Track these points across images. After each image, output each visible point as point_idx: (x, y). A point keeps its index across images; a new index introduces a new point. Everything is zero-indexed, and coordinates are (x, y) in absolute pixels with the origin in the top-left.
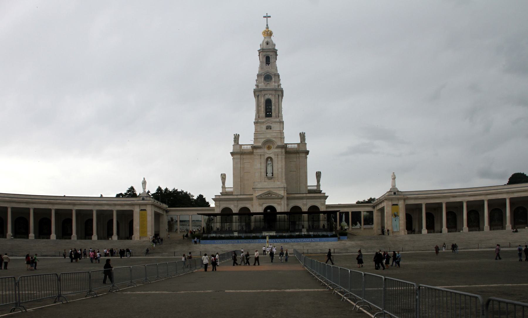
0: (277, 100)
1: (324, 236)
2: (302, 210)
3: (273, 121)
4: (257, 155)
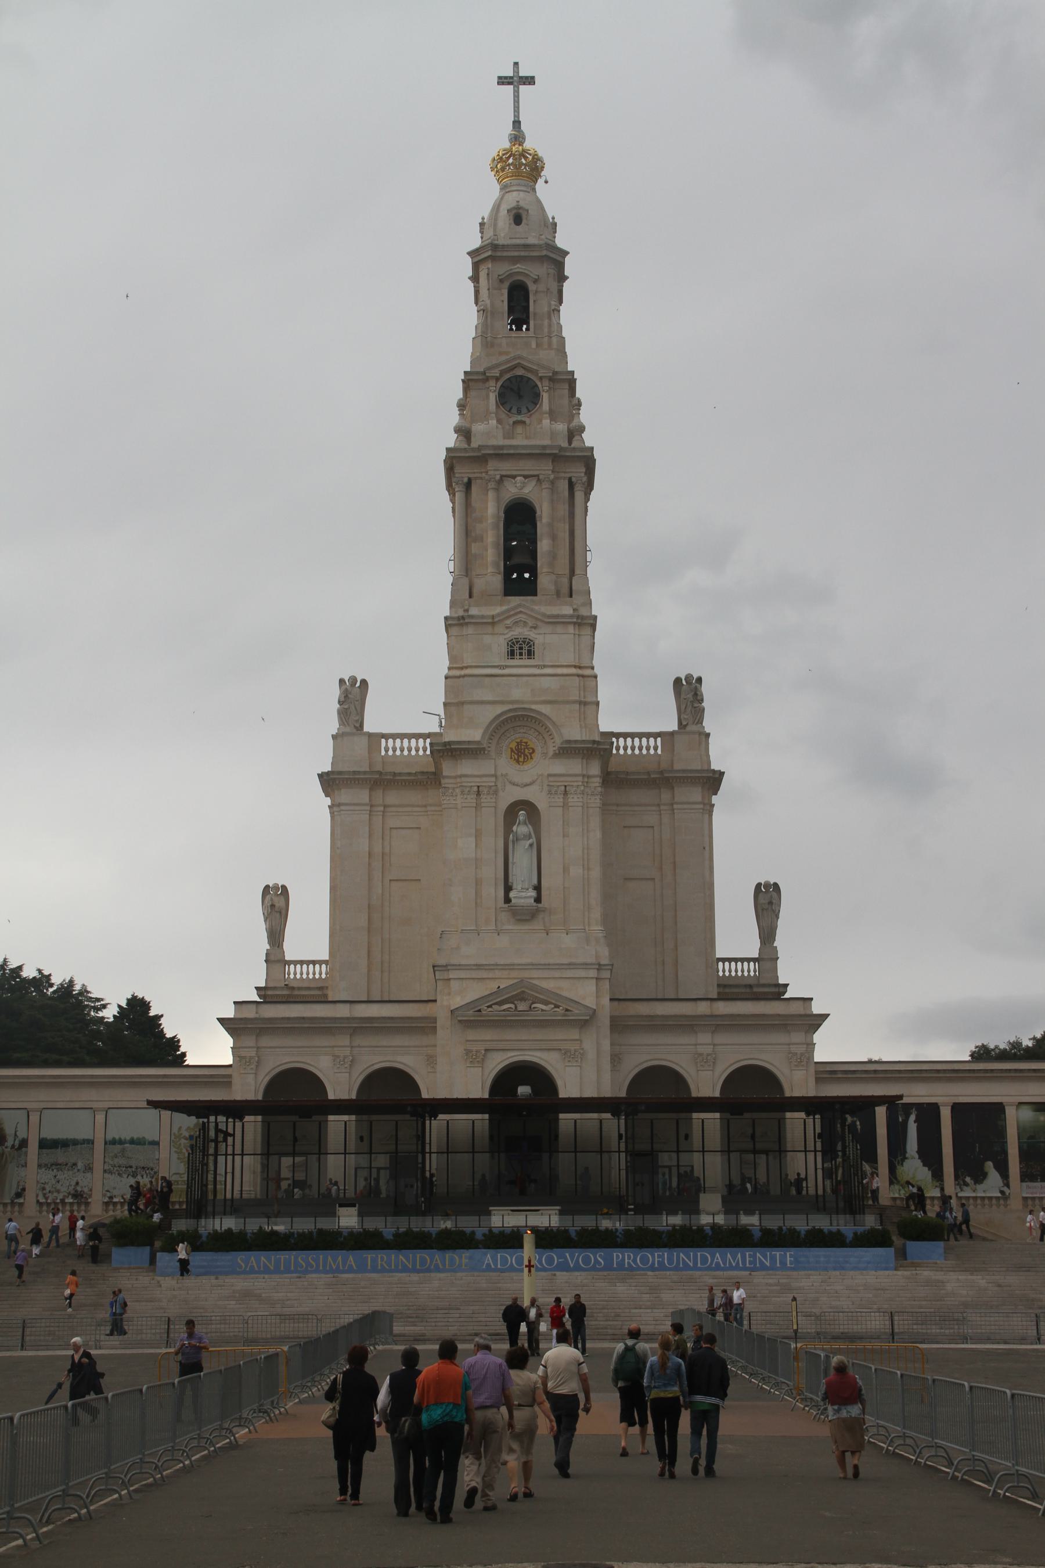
0: (563, 509)
1: (818, 1239)
2: (692, 1087)
3: (544, 615)
4: (458, 790)
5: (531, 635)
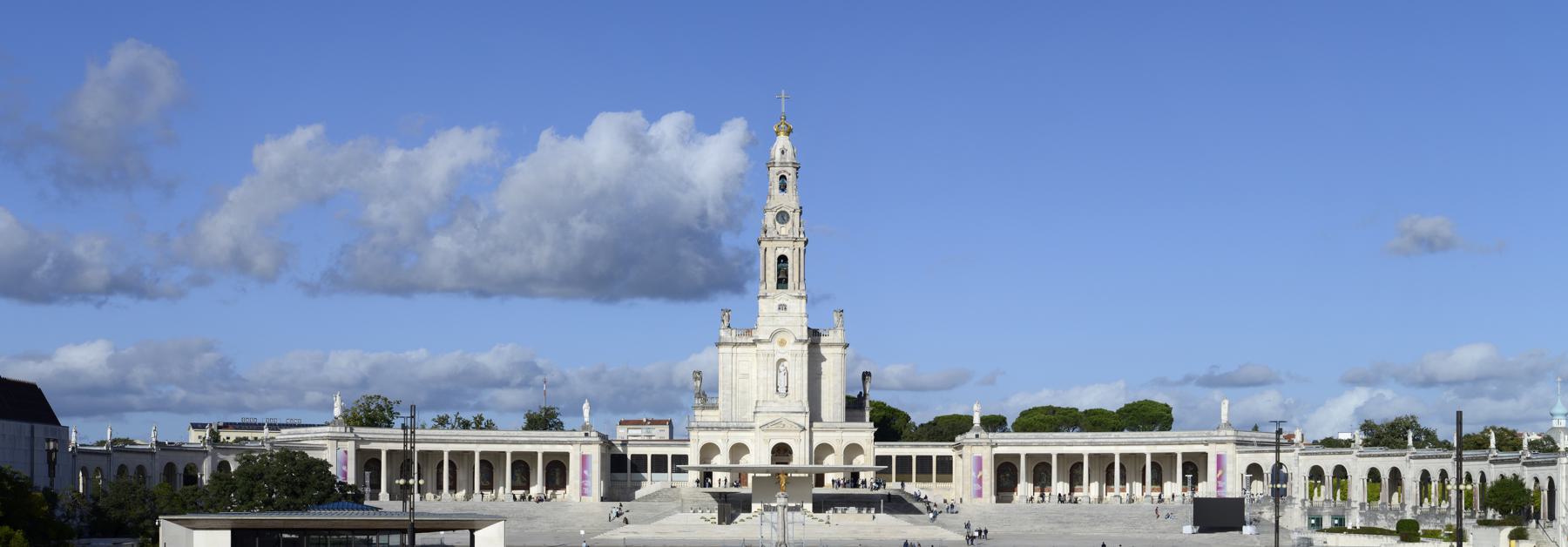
0: (796, 259)
5: (785, 302)
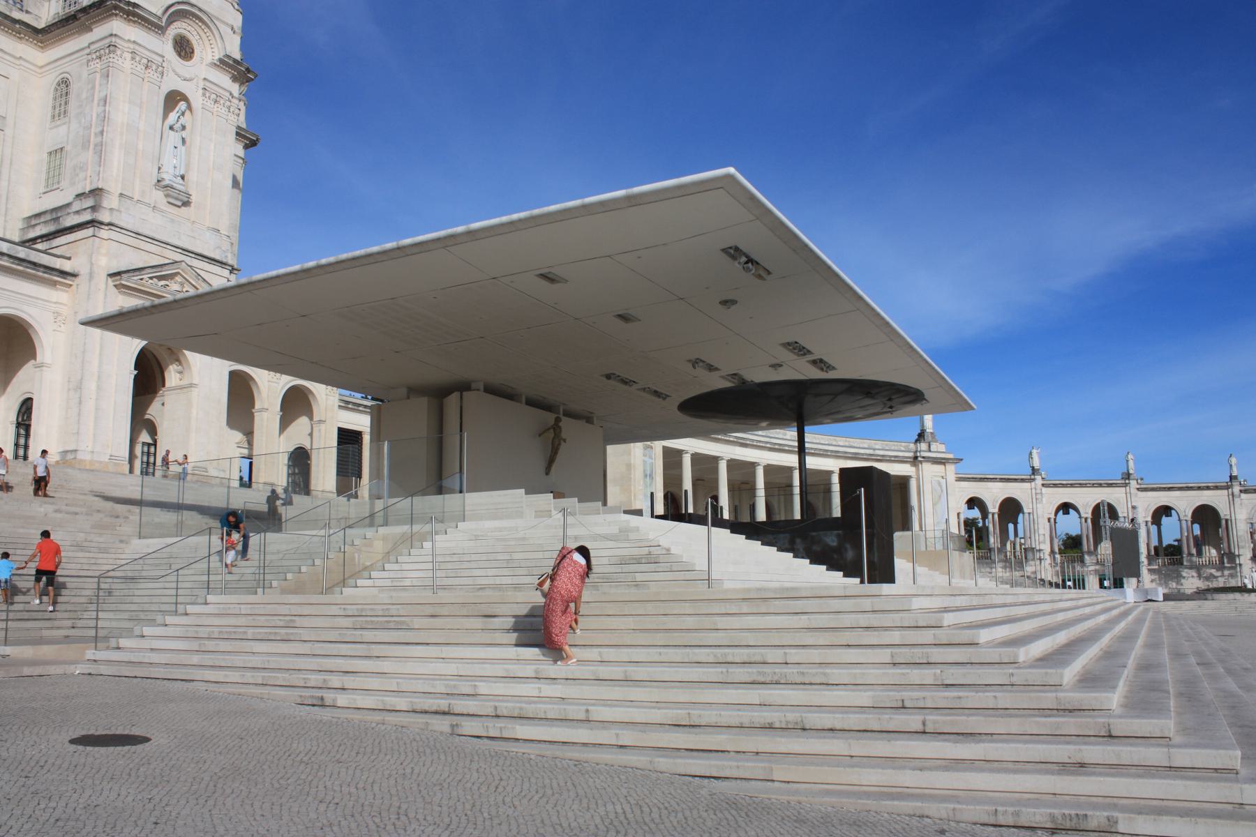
4: (128, 56)
